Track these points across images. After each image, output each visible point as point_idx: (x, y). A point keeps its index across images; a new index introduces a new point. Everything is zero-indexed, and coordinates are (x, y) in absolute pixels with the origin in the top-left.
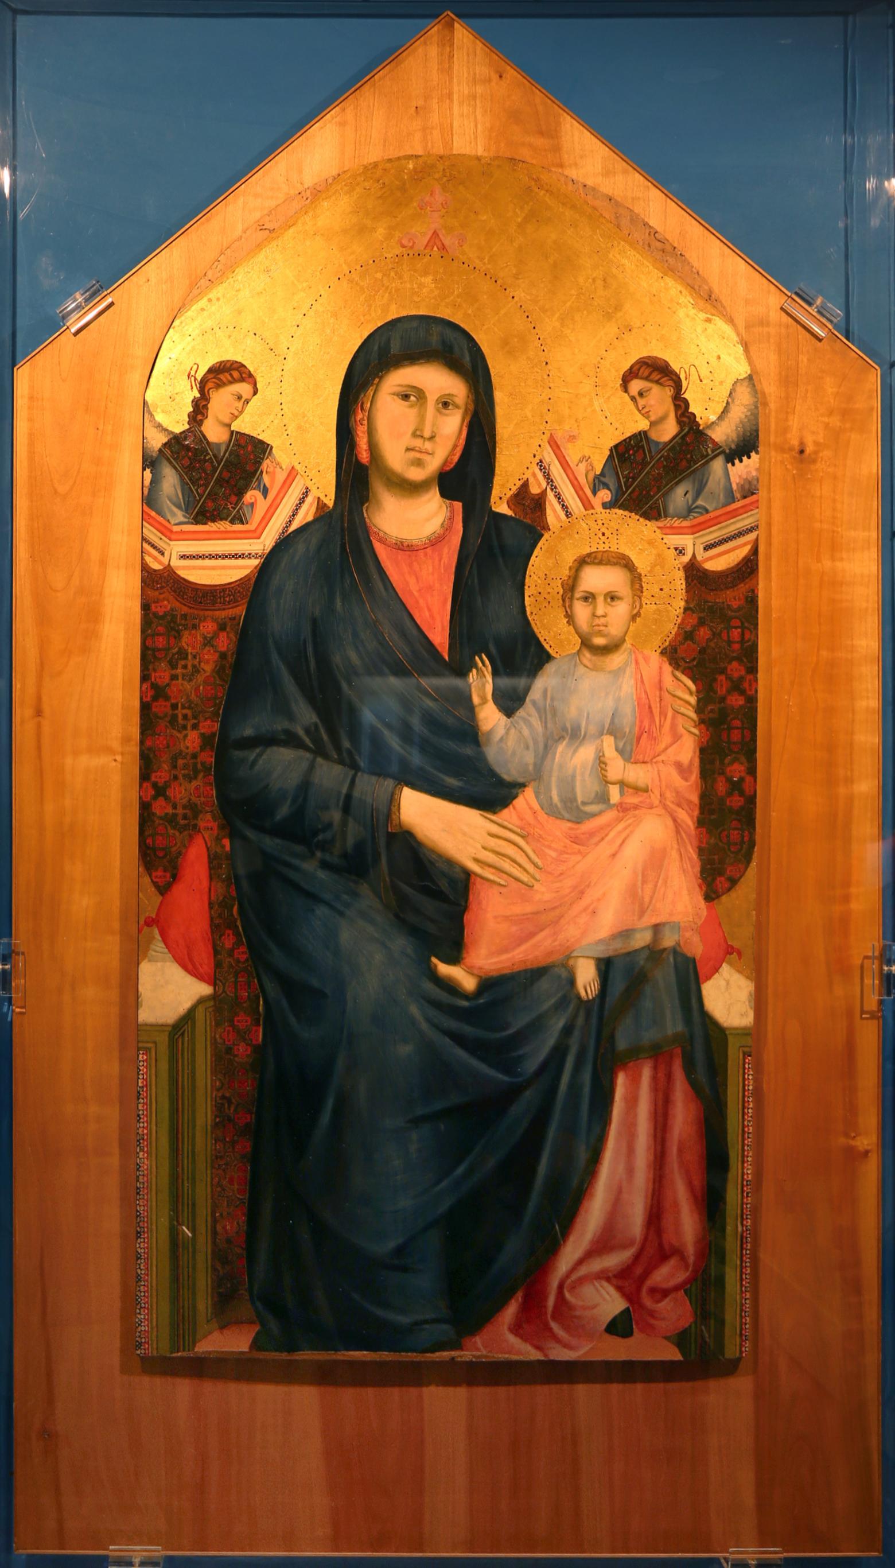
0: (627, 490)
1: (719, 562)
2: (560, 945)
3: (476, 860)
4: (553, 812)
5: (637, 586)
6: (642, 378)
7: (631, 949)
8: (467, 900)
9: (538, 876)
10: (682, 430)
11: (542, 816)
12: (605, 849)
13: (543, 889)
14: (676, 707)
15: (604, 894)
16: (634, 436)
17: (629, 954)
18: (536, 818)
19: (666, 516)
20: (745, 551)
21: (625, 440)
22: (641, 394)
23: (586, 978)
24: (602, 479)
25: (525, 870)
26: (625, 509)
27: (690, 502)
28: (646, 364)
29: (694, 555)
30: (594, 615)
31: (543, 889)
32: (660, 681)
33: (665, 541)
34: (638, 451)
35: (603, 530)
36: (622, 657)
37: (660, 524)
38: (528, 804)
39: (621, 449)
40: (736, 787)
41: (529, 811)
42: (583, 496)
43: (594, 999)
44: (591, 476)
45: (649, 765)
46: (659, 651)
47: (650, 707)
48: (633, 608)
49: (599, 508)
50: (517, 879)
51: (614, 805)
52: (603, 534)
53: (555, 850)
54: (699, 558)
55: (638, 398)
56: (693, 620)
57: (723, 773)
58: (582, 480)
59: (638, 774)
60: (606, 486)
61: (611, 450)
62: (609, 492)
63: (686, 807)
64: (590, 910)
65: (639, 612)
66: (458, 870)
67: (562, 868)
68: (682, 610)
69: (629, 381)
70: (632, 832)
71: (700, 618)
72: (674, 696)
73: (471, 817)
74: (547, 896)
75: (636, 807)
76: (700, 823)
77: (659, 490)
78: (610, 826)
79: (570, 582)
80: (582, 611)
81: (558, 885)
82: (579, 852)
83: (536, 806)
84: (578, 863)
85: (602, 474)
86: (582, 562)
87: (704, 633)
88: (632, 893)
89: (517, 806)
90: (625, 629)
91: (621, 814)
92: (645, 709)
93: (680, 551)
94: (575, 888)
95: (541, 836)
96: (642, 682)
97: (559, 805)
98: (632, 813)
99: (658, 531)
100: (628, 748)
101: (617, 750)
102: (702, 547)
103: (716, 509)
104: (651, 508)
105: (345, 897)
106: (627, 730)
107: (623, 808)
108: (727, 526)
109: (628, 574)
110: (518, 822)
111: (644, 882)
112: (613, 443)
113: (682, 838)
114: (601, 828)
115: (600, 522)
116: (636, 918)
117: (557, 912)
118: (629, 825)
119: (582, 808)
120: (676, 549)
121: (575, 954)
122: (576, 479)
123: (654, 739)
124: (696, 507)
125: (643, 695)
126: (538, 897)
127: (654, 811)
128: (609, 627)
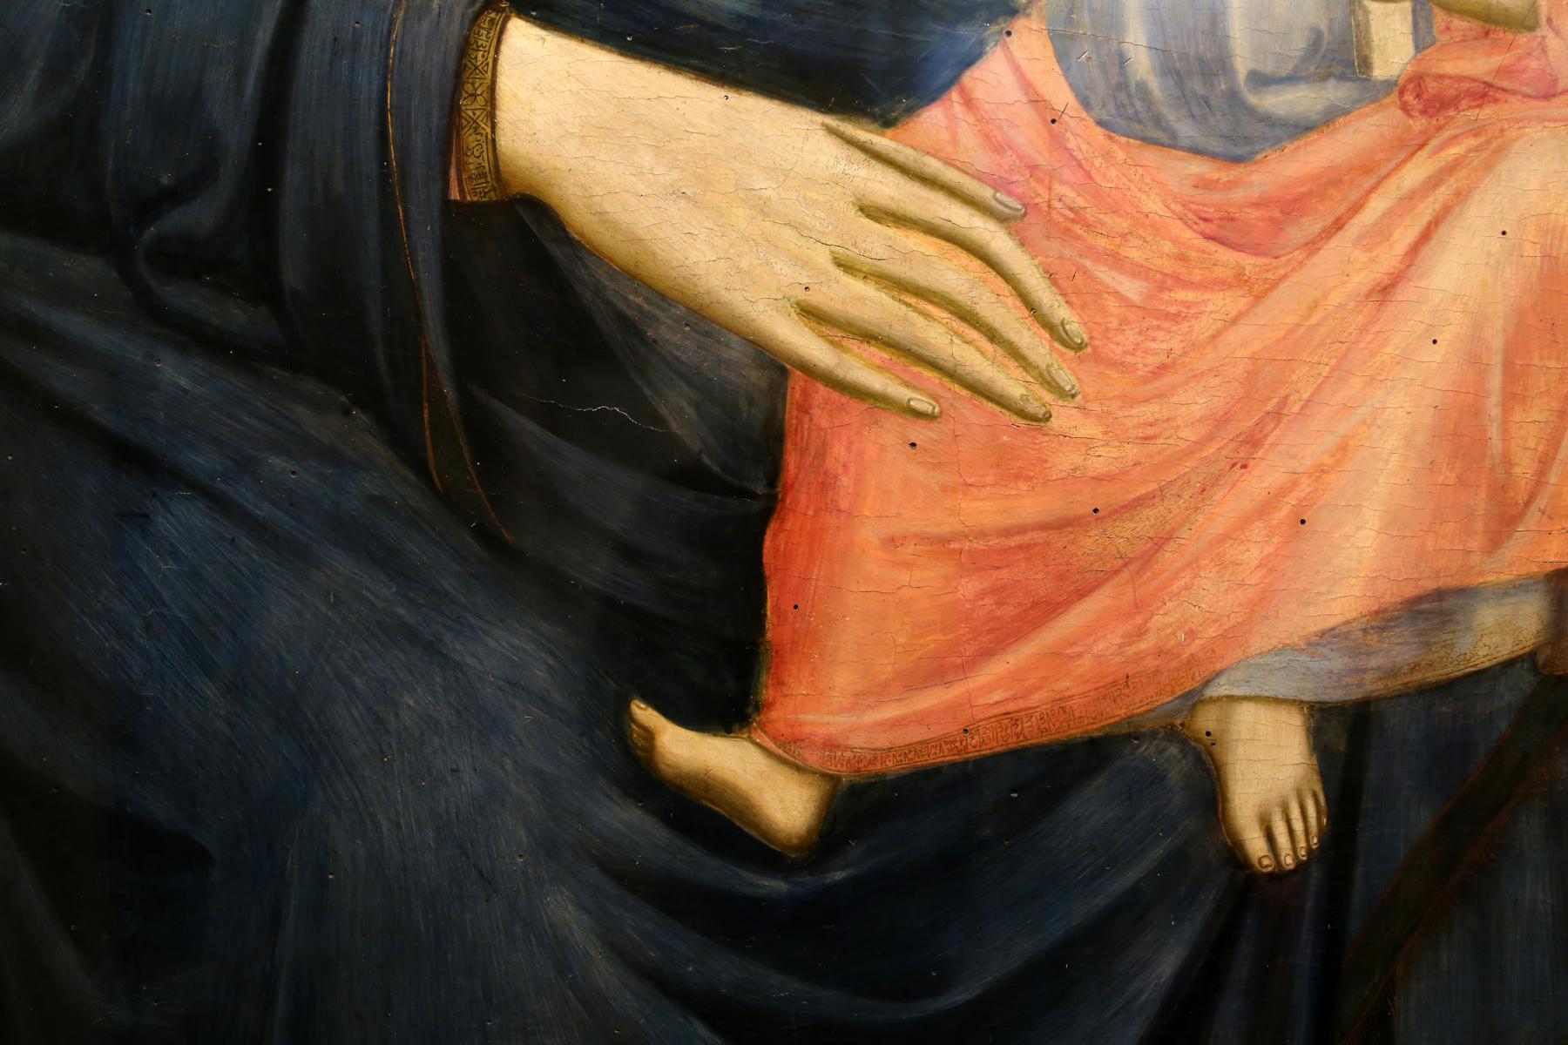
2: (1160, 653)
3: (812, 314)
4: (1128, 115)
7: (1455, 670)
8: (774, 473)
9: (1066, 378)
11: (1084, 135)
12: (1344, 268)
13: (1090, 429)
15: (1343, 449)
17: (1447, 687)
18: (1058, 142)
23: (1269, 781)
25: (1014, 353)
31: (1090, 429)
38: (1026, 85)
41: (1028, 114)
43: (1301, 866)
50: (980, 390)
51: (1389, 85)
53: (1138, 271)
64: (1283, 513)
66: (736, 352)
67: (1167, 342)
70: (1461, 196)
73: (789, 142)
74: (1104, 459)
75: (1484, 93)
78: (1368, 171)
81: (1151, 411)
82: (1240, 280)
83: (1060, 94)
84: (1234, 322)
88: (1460, 438)
89: (979, 93)
91: (1419, 124)
94: (1221, 421)
95: (1078, 216)
97: (1154, 85)
98: (1469, 115)
105: (277, 463)
107: (1428, 99)
110: (982, 160)
111: (1513, 397)
114: (1330, 181)
116: (1475, 544)
117: (1145, 522)
118: (1451, 168)
119: (1253, 99)
121: (1220, 689)
126: (1065, 461)
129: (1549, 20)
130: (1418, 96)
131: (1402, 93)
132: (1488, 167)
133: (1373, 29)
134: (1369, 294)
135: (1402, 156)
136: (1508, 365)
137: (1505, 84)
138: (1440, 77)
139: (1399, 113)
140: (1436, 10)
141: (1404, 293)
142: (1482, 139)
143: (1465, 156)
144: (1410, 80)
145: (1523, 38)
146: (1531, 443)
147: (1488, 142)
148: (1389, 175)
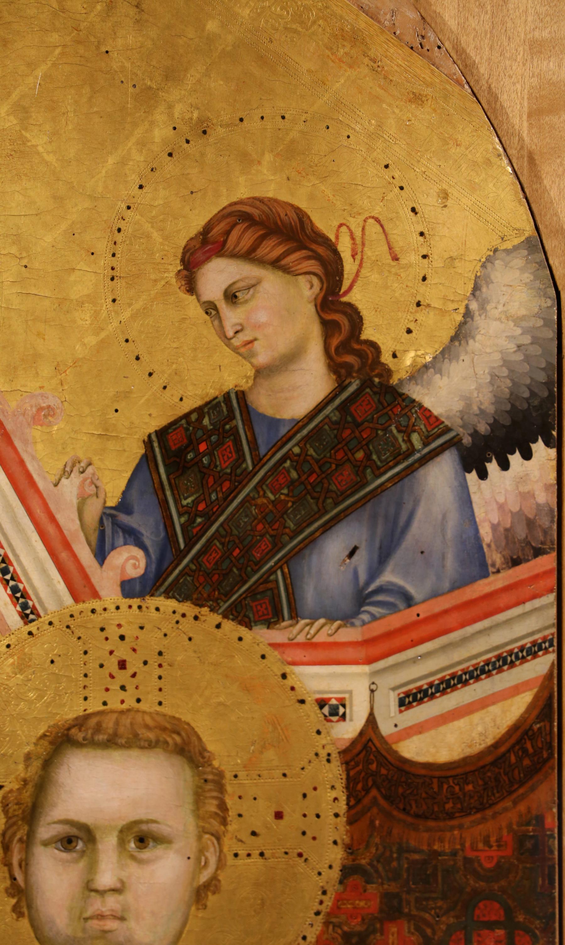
0: (190, 545)
1: (442, 740)
5: (212, 806)
6: (234, 256)
10: (341, 387)
16: (210, 406)
19: (295, 615)
20: (517, 708)
21: (187, 416)
22: (231, 297)
24: (123, 518)
26: (183, 598)
27: (363, 577)
28: (246, 217)
29: (371, 721)
30: (89, 888)
33: (289, 682)
34: (220, 443)
35: (123, 652)
37: (277, 635)
39: (176, 440)
42: (70, 566)
44: (93, 511)
49: (110, 594)
52: (122, 665)
54: (386, 728)
55: (222, 306)
56: (369, 902)
58: (69, 521)
60: (133, 537)
61: (148, 443)
62: (139, 553)
65: (214, 878)
68: (335, 874)
69: (199, 264)
71: (387, 896)
77: (277, 546)
79: (27, 796)
80: (54, 878)
85: (124, 506)
86: (63, 740)
90: (175, 925)
93: (334, 710)
99: (273, 655)
102: (393, 699)
103: (435, 595)
104: (252, 593)
108: (465, 640)
109: (188, 773)
112: (155, 424)
115: (113, 632)
122: (53, 519)
124: (380, 590)
128: (132, 923)
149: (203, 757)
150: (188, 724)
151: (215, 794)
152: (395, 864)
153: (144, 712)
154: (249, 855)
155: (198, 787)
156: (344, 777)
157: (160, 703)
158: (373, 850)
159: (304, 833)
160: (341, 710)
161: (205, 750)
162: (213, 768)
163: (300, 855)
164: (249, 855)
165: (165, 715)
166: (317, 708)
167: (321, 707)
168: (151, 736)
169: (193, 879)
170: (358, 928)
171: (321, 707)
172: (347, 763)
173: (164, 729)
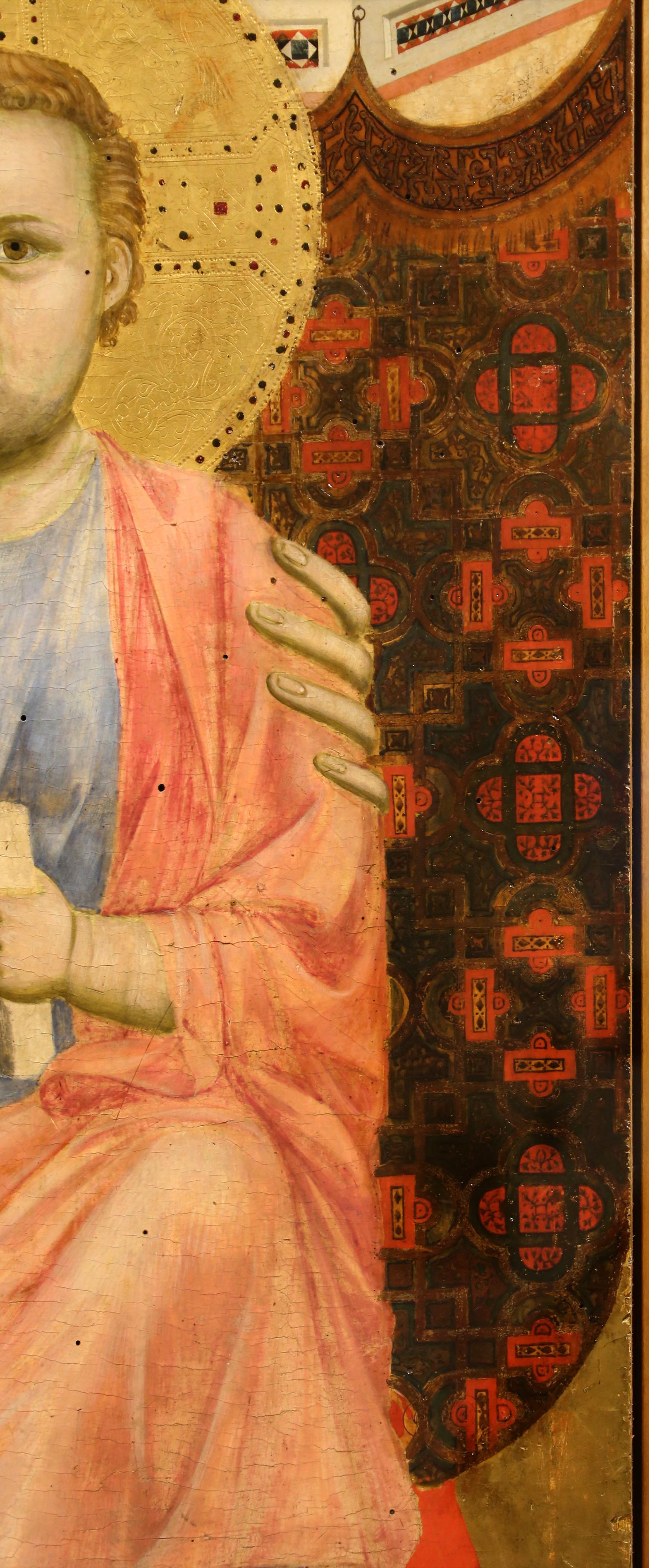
5: (119, 195)
14: (288, 685)
32: (220, 582)
36: (61, 484)
40: (541, 1002)
45: (176, 921)
46: (215, 457)
47: (178, 688)
48: (106, 283)
51: (30, 1085)
56: (356, 332)
57: (483, 950)
59: (130, 959)
63: (329, 1087)
68: (307, 293)
70: (103, 1195)
71: (383, 324)
72: (278, 640)
75: (123, 1092)
76: (394, 1153)
87: (399, 384)
90: (70, 370)
91: (60, 1123)
92: (155, 691)
96: (145, 584)
100: (88, 853)
101: (41, 860)
106: (84, 779)
107: (70, 1099)
109: (81, 146)
111: (157, 1399)
113: (316, 1218)
118: (93, 1167)
120: (281, 40)
123: (194, 816)
125: (151, 642)
127: (196, 1107)
129: (185, 1022)
130: (59, 1096)
131: (43, 1092)
132: (129, 1166)
133: (14, 1030)
134: (12, 1295)
135: (45, 1154)
136: (150, 1367)
137: (144, 1084)
138: (81, 1077)
139: (41, 1113)
140: (75, 1011)
141: (47, 1293)
142: (122, 1138)
143: (106, 1156)
144: (51, 1080)
145: (160, 1039)
146: (174, 1447)
147: (128, 1141)
148: (31, 1174)
149: (104, 123)
150: (79, 73)
151: (123, 177)
152: (394, 276)
153: (11, 54)
154: (177, 267)
155: (97, 167)
156: (317, 150)
157: (35, 41)
158: (363, 257)
159: (259, 234)
160: (311, 50)
161: (106, 111)
162: (119, 138)
163: (254, 266)
164: (177, 267)
165: (42, 59)
166: (274, 46)
167: (281, 46)
168: (23, 90)
169: (95, 302)
170: (341, 370)
171: (281, 46)
172: (321, 130)
173: (43, 80)
